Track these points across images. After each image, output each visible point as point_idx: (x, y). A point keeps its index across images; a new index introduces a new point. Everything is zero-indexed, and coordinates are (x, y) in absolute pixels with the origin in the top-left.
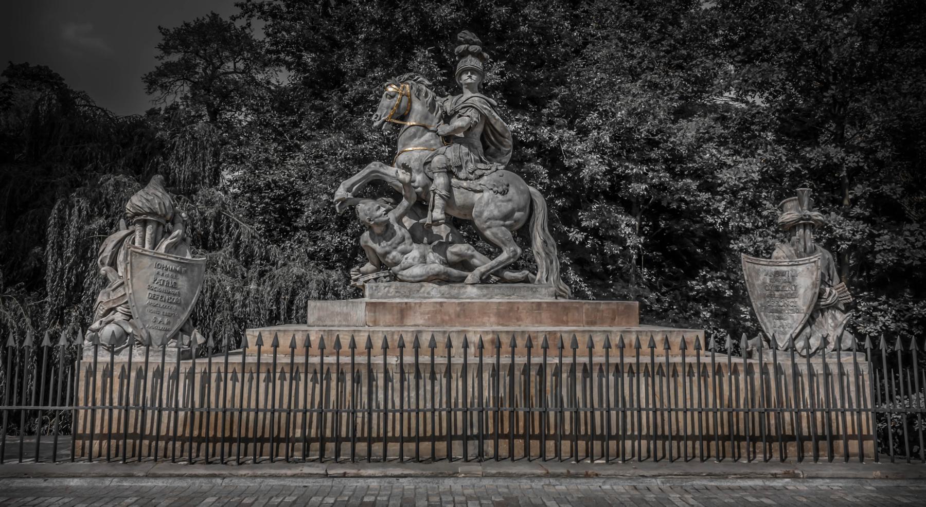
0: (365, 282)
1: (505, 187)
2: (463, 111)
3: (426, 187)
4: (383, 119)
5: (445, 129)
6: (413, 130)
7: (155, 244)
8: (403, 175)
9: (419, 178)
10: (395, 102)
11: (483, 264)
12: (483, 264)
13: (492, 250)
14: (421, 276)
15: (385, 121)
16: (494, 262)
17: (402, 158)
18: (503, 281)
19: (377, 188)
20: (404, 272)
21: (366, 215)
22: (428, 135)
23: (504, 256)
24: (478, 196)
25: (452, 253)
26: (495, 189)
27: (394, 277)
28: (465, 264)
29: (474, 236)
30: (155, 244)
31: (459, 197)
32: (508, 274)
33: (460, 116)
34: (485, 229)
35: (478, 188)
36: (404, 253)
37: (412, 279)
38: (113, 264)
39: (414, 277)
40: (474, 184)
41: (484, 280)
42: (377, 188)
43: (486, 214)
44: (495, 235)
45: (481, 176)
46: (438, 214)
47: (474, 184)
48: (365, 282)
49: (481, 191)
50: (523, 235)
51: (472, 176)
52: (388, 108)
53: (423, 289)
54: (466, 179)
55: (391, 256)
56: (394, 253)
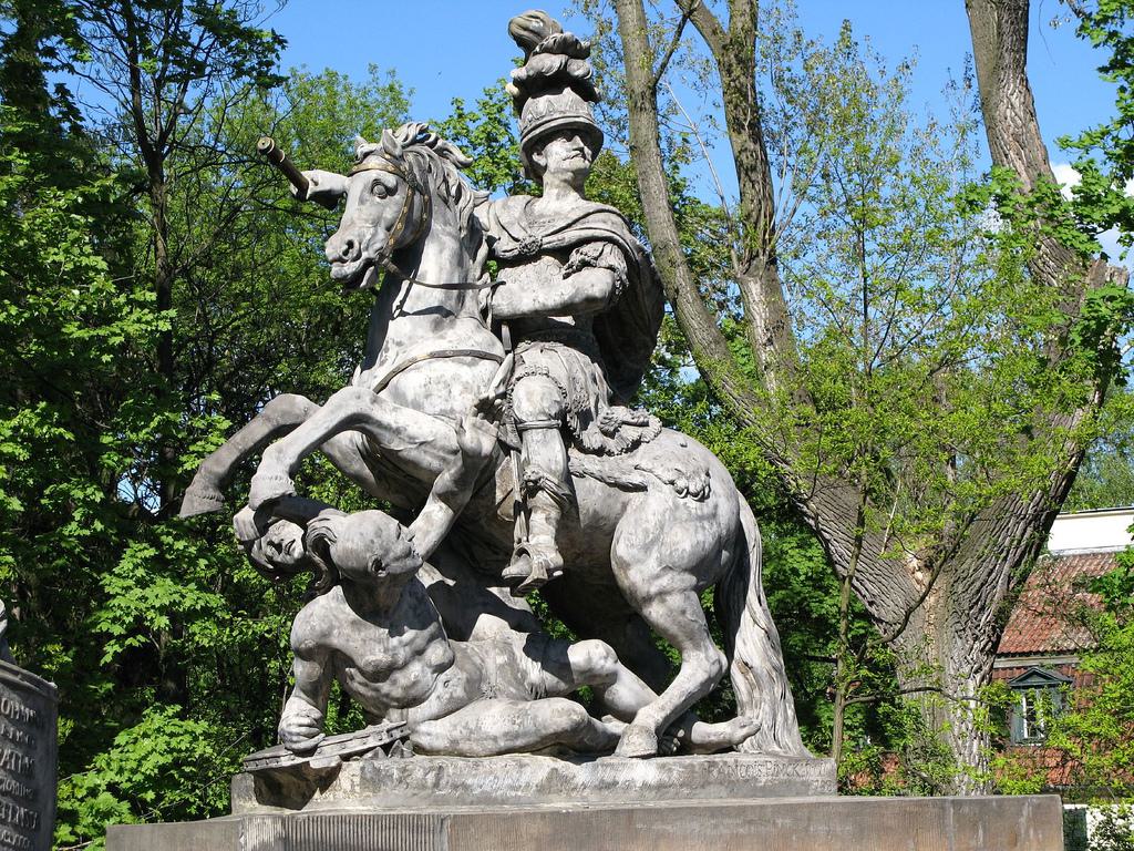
0: (347, 758)
1: (703, 476)
2: (590, 250)
15: (369, 263)
18: (687, 748)
26: (681, 483)
33: (585, 264)
34: (649, 599)
35: (636, 479)
40: (620, 467)
45: (636, 444)
48: (347, 758)
49: (641, 488)
51: (611, 444)
52: (376, 223)
54: (600, 452)
55: (402, 679)
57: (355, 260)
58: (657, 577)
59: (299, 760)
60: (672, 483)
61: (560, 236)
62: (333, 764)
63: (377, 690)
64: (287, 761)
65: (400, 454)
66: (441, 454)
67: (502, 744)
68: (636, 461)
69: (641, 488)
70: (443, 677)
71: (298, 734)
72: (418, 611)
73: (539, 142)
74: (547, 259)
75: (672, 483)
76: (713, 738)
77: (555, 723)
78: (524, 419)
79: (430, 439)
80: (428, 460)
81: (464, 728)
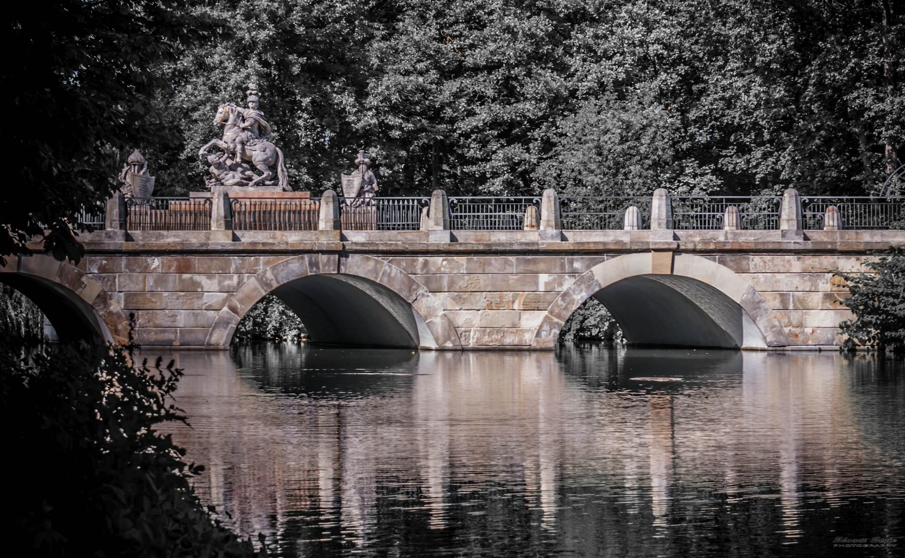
3: (234, 148)
5: (242, 125)
7: (138, 172)
8: (225, 146)
9: (232, 146)
10: (222, 115)
11: (256, 178)
12: (256, 178)
13: (260, 173)
16: (260, 178)
17: (225, 138)
18: (264, 185)
19: (215, 149)
22: (236, 128)
23: (264, 176)
27: (222, 184)
28: (250, 179)
29: (253, 168)
30: (138, 172)
31: (248, 153)
32: (267, 183)
38: (125, 178)
41: (257, 184)
42: (215, 149)
46: (238, 160)
47: (253, 148)
50: (273, 168)
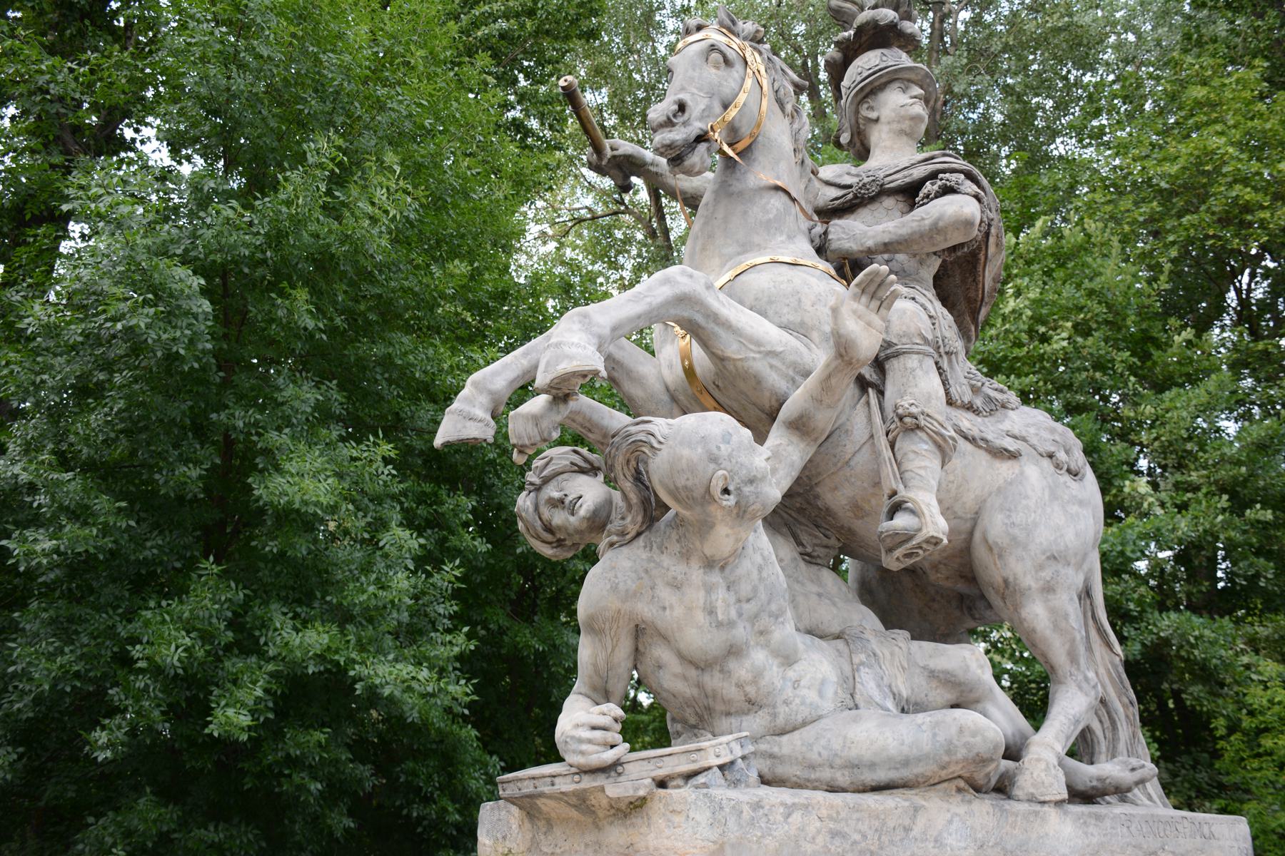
0: (662, 784)
4: (696, 127)
6: (778, 201)
14: (906, 763)
15: (702, 138)
20: (787, 745)
21: (714, 459)
24: (1005, 469)
25: (932, 674)
26: (1062, 456)
33: (948, 190)
36: (788, 660)
37: (842, 778)
39: (853, 766)
43: (1043, 537)
44: (1058, 618)
48: (662, 784)
49: (1013, 456)
53: (921, 821)
54: (969, 408)
55: (741, 670)
56: (759, 656)
57: (685, 124)
58: (1041, 567)
59: (587, 783)
60: (1051, 456)
61: (905, 173)
62: (642, 793)
63: (699, 686)
64: (565, 786)
65: (739, 364)
66: (791, 373)
67: (882, 776)
68: (1006, 425)
69: (1013, 456)
70: (791, 674)
71: (590, 741)
72: (764, 574)
73: (872, 89)
74: (889, 202)
75: (1051, 456)
76: (1095, 783)
77: (966, 744)
78: (894, 341)
79: (780, 349)
80: (775, 380)
81: (824, 748)
